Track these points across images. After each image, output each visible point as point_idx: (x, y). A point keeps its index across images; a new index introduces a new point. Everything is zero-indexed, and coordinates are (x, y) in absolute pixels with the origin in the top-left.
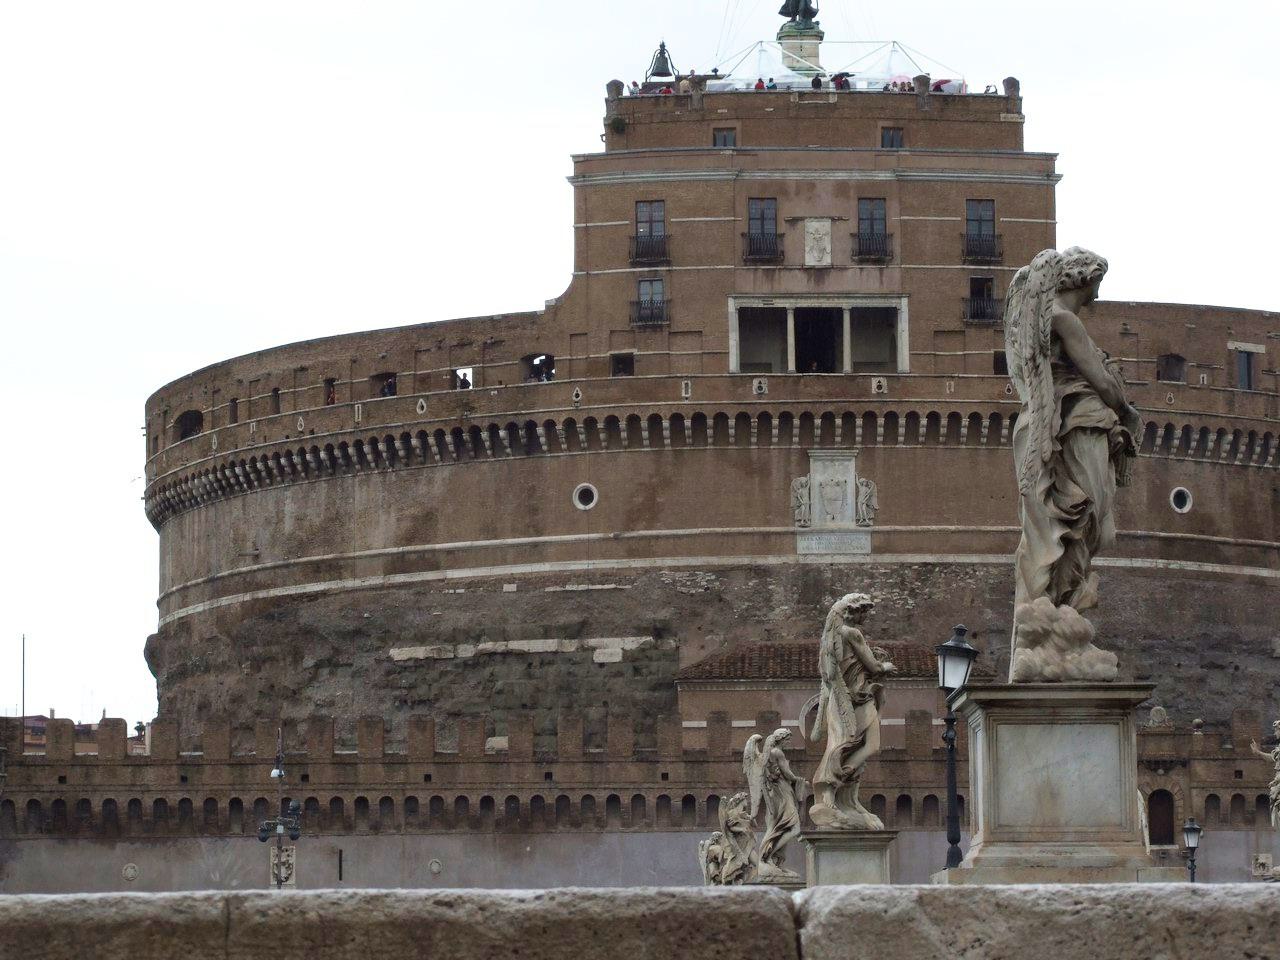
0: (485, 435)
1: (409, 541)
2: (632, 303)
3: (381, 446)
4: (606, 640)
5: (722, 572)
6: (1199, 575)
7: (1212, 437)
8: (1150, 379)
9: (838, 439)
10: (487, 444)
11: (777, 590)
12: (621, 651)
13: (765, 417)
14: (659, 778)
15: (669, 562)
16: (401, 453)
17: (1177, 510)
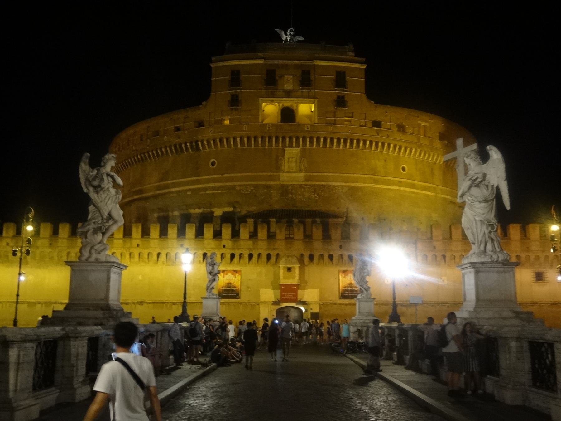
0: (183, 146)
1: (161, 180)
2: (229, 101)
3: (154, 152)
4: (218, 210)
5: (256, 187)
6: (410, 192)
7: (414, 150)
8: (395, 129)
9: (294, 145)
10: (184, 149)
11: (274, 193)
12: (222, 212)
13: (270, 138)
14: (222, 247)
15: (239, 183)
16: (160, 153)
17: (403, 172)
